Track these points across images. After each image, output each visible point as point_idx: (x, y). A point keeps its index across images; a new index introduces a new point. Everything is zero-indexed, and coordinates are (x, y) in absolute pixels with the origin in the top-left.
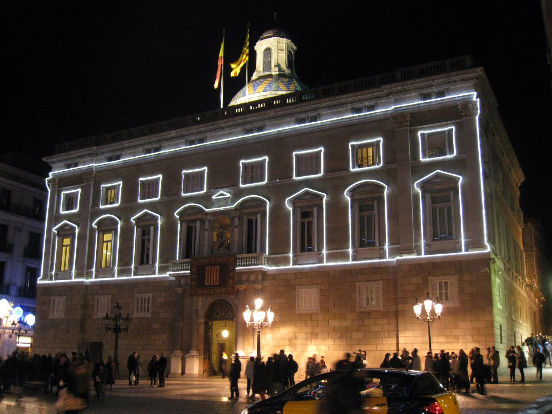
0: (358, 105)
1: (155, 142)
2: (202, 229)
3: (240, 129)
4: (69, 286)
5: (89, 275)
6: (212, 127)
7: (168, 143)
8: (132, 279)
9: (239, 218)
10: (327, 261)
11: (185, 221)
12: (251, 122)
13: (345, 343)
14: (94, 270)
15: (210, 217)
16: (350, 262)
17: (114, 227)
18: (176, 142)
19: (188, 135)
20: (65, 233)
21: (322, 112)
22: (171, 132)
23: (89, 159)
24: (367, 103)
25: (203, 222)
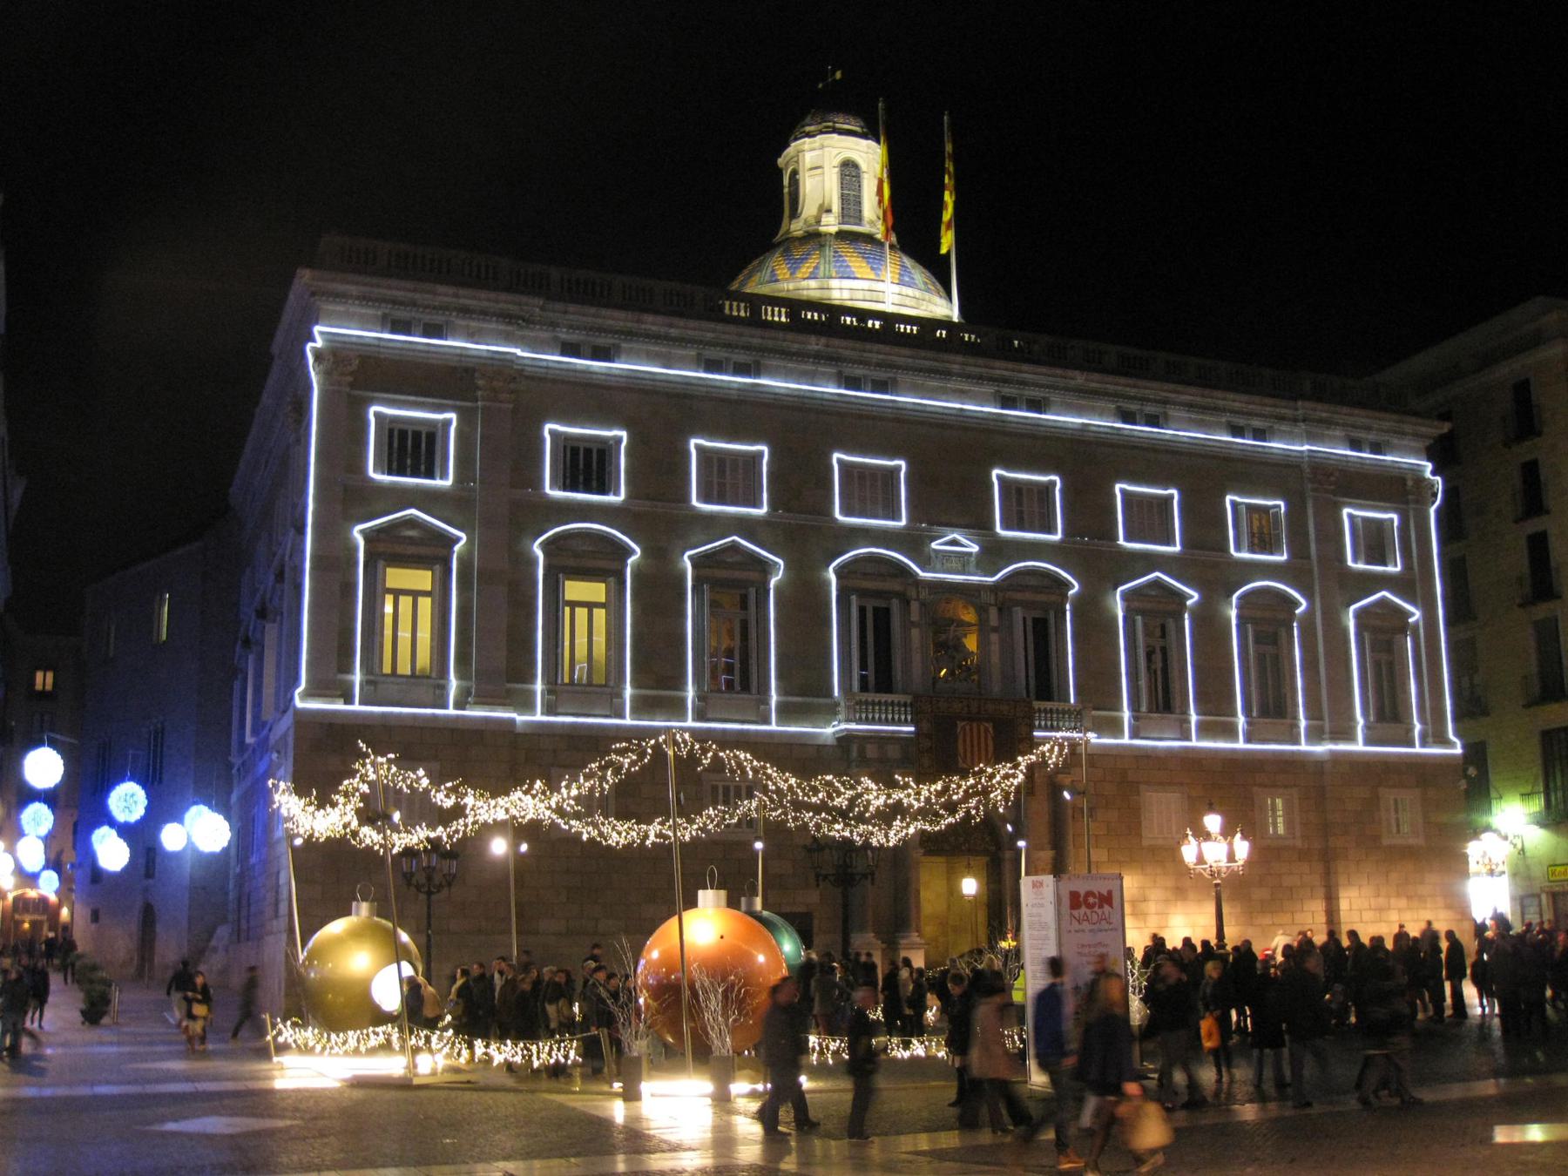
0: (1241, 421)
1: (748, 348)
2: (908, 625)
3: (989, 389)
4: (453, 731)
5: (526, 704)
6: (928, 363)
7: (782, 363)
8: (448, 718)
9: (1000, 610)
10: (1198, 739)
11: (863, 593)
12: (1023, 383)
13: (1239, 910)
14: (539, 686)
15: (924, 594)
16: (1241, 745)
17: (615, 566)
18: (811, 367)
19: (854, 362)
20: (399, 549)
21: (1173, 412)
22: (813, 339)
23: (493, 326)
24: (1257, 423)
25: (906, 602)
